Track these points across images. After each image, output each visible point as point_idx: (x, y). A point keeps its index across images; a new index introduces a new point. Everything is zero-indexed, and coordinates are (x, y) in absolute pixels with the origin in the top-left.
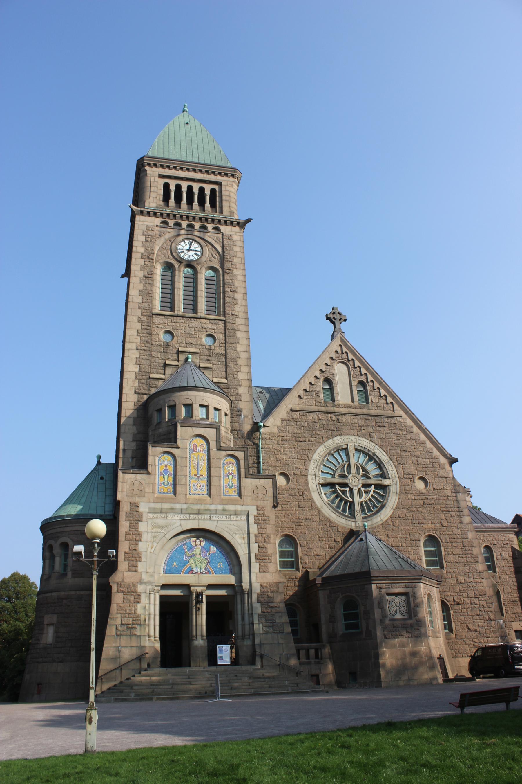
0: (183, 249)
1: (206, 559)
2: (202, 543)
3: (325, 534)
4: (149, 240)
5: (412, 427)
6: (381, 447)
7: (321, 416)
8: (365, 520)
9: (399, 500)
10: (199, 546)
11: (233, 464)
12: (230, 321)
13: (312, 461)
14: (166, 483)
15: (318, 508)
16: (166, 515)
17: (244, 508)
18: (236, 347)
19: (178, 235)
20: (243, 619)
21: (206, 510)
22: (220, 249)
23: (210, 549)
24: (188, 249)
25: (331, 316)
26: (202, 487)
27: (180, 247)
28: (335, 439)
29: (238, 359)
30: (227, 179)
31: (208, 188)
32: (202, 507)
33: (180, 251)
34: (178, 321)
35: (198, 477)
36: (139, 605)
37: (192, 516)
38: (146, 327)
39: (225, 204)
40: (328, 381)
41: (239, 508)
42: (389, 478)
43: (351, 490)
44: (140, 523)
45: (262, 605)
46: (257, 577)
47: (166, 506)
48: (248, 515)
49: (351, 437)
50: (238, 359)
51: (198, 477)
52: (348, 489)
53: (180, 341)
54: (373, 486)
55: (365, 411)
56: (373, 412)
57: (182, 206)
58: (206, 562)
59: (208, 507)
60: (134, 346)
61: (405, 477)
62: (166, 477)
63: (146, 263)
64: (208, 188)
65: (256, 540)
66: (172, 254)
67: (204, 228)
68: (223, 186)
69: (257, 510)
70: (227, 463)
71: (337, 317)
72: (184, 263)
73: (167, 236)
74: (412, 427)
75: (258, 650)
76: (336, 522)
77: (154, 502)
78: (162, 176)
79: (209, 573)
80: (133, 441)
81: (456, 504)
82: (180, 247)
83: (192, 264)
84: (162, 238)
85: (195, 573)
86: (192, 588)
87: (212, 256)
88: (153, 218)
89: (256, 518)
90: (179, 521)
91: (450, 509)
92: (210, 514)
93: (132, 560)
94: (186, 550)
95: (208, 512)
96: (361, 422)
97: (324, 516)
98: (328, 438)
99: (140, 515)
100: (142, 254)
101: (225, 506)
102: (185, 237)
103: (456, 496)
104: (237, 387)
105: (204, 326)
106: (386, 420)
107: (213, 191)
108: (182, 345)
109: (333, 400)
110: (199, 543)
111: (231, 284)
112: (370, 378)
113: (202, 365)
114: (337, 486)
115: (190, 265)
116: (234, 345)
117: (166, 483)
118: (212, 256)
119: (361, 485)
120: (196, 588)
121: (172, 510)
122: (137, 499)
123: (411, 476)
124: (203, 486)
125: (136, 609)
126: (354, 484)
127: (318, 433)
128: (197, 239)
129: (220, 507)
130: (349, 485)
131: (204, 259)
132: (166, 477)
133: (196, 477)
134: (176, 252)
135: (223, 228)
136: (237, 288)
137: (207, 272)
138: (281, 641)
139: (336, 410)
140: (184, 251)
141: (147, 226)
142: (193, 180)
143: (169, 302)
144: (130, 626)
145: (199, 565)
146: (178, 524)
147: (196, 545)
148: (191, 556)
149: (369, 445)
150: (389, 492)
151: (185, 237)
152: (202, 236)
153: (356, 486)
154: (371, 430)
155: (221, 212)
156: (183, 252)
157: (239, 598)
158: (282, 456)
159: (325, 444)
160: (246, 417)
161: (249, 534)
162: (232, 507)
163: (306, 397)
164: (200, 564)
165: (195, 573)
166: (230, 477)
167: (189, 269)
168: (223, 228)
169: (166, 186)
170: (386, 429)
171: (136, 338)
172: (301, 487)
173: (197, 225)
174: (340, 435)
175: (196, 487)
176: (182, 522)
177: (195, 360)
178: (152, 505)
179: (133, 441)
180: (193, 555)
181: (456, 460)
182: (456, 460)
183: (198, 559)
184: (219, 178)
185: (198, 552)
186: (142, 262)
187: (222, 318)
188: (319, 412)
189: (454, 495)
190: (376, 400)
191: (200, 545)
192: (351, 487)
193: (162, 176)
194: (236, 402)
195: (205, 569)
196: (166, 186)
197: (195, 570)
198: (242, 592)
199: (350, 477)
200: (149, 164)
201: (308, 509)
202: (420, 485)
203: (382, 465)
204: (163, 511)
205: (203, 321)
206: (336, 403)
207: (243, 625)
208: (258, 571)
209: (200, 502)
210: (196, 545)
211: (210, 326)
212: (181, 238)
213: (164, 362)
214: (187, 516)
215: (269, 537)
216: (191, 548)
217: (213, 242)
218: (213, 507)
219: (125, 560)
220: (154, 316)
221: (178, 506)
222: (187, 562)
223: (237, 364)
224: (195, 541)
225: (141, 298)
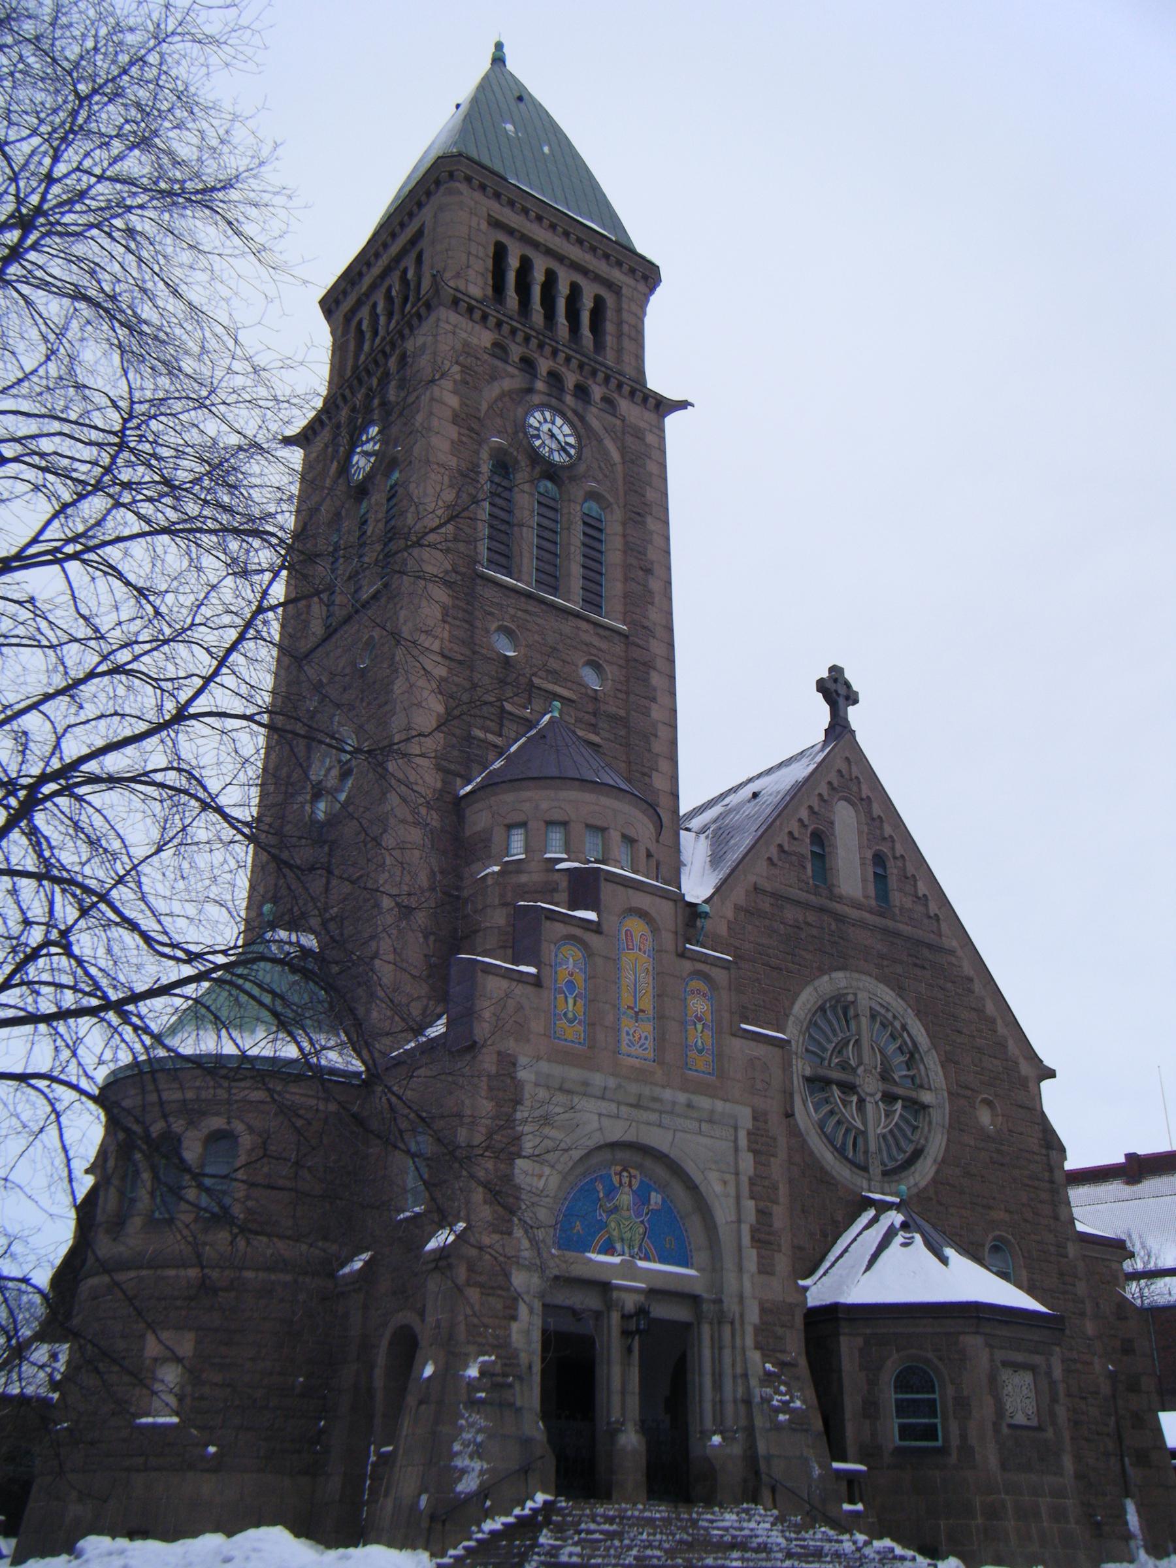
0: (537, 429)
1: (642, 1222)
2: (634, 1181)
4: (468, 378)
5: (970, 980)
6: (918, 1014)
7: (811, 917)
8: (886, 1179)
9: (947, 1145)
10: (627, 1189)
11: (704, 995)
13: (792, 1018)
14: (570, 1015)
15: (800, 1134)
16: (569, 1097)
18: (648, 709)
19: (530, 390)
20: (718, 1385)
21: (655, 1099)
23: (649, 1200)
24: (552, 432)
25: (831, 686)
26: (642, 1041)
27: (532, 421)
28: (835, 975)
29: (652, 738)
30: (631, 282)
32: (647, 1091)
33: (532, 432)
36: (515, 1326)
37: (623, 1109)
38: (461, 604)
39: (626, 343)
40: (819, 838)
41: (719, 1105)
42: (930, 1089)
43: (861, 1102)
47: (574, 1074)
48: (736, 1129)
49: (864, 977)
50: (652, 738)
51: (637, 1013)
52: (855, 1099)
54: (900, 1102)
58: (641, 1230)
59: (658, 1091)
60: (436, 647)
61: (959, 1093)
62: (571, 1001)
63: (464, 439)
65: (751, 1191)
69: (755, 1119)
70: (692, 992)
71: (842, 691)
73: (507, 384)
75: (763, 1467)
76: (834, 1173)
77: (549, 1060)
78: (496, 224)
80: (433, 889)
81: (1047, 1174)
84: (496, 384)
86: (615, 1294)
87: (600, 467)
88: (477, 327)
90: (596, 1117)
91: (1036, 1183)
92: (661, 1112)
94: (601, 1195)
95: (657, 1106)
97: (812, 1154)
98: (822, 971)
99: (518, 1085)
101: (692, 1097)
102: (545, 399)
103: (1048, 1155)
105: (585, 637)
106: (926, 952)
107: (599, 301)
110: (627, 1180)
114: (834, 1087)
115: (551, 472)
118: (600, 467)
119: (879, 1096)
120: (624, 1295)
121: (585, 1089)
122: (511, 1045)
123: (969, 1093)
124: (646, 1038)
125: (509, 1336)
126: (868, 1090)
127: (803, 953)
128: (570, 414)
129: (682, 1098)
130: (859, 1090)
131: (582, 468)
132: (571, 1001)
133: (630, 1012)
134: (525, 433)
135: (624, 405)
136: (652, 563)
137: (586, 505)
139: (838, 907)
141: (466, 344)
144: (500, 1379)
145: (628, 1235)
146: (596, 1125)
147: (621, 1184)
149: (894, 1004)
150: (930, 1123)
151: (545, 399)
152: (580, 410)
153: (872, 1095)
156: (538, 437)
157: (706, 1330)
159: (816, 983)
161: (737, 1174)
162: (704, 1102)
163: (780, 863)
166: (699, 1027)
167: (549, 485)
169: (500, 253)
174: (843, 968)
176: (606, 1122)
177: (567, 718)
180: (616, 1209)
181: (1051, 1074)
182: (1051, 1074)
183: (626, 1219)
184: (616, 275)
185: (626, 1203)
186: (453, 432)
188: (807, 906)
189: (1044, 1151)
190: (908, 903)
191: (630, 1185)
192: (863, 1095)
193: (496, 224)
195: (640, 1249)
196: (500, 253)
198: (721, 1318)
199: (860, 1070)
200: (468, 179)
202: (985, 1117)
203: (917, 1056)
204: (566, 1086)
205: (584, 625)
207: (719, 1404)
209: (641, 1076)
210: (621, 1184)
211: (596, 641)
212: (536, 399)
214: (613, 1107)
215: (775, 1188)
216: (611, 1191)
220: (478, 581)
221: (598, 1079)
223: (649, 751)
224: (620, 1174)
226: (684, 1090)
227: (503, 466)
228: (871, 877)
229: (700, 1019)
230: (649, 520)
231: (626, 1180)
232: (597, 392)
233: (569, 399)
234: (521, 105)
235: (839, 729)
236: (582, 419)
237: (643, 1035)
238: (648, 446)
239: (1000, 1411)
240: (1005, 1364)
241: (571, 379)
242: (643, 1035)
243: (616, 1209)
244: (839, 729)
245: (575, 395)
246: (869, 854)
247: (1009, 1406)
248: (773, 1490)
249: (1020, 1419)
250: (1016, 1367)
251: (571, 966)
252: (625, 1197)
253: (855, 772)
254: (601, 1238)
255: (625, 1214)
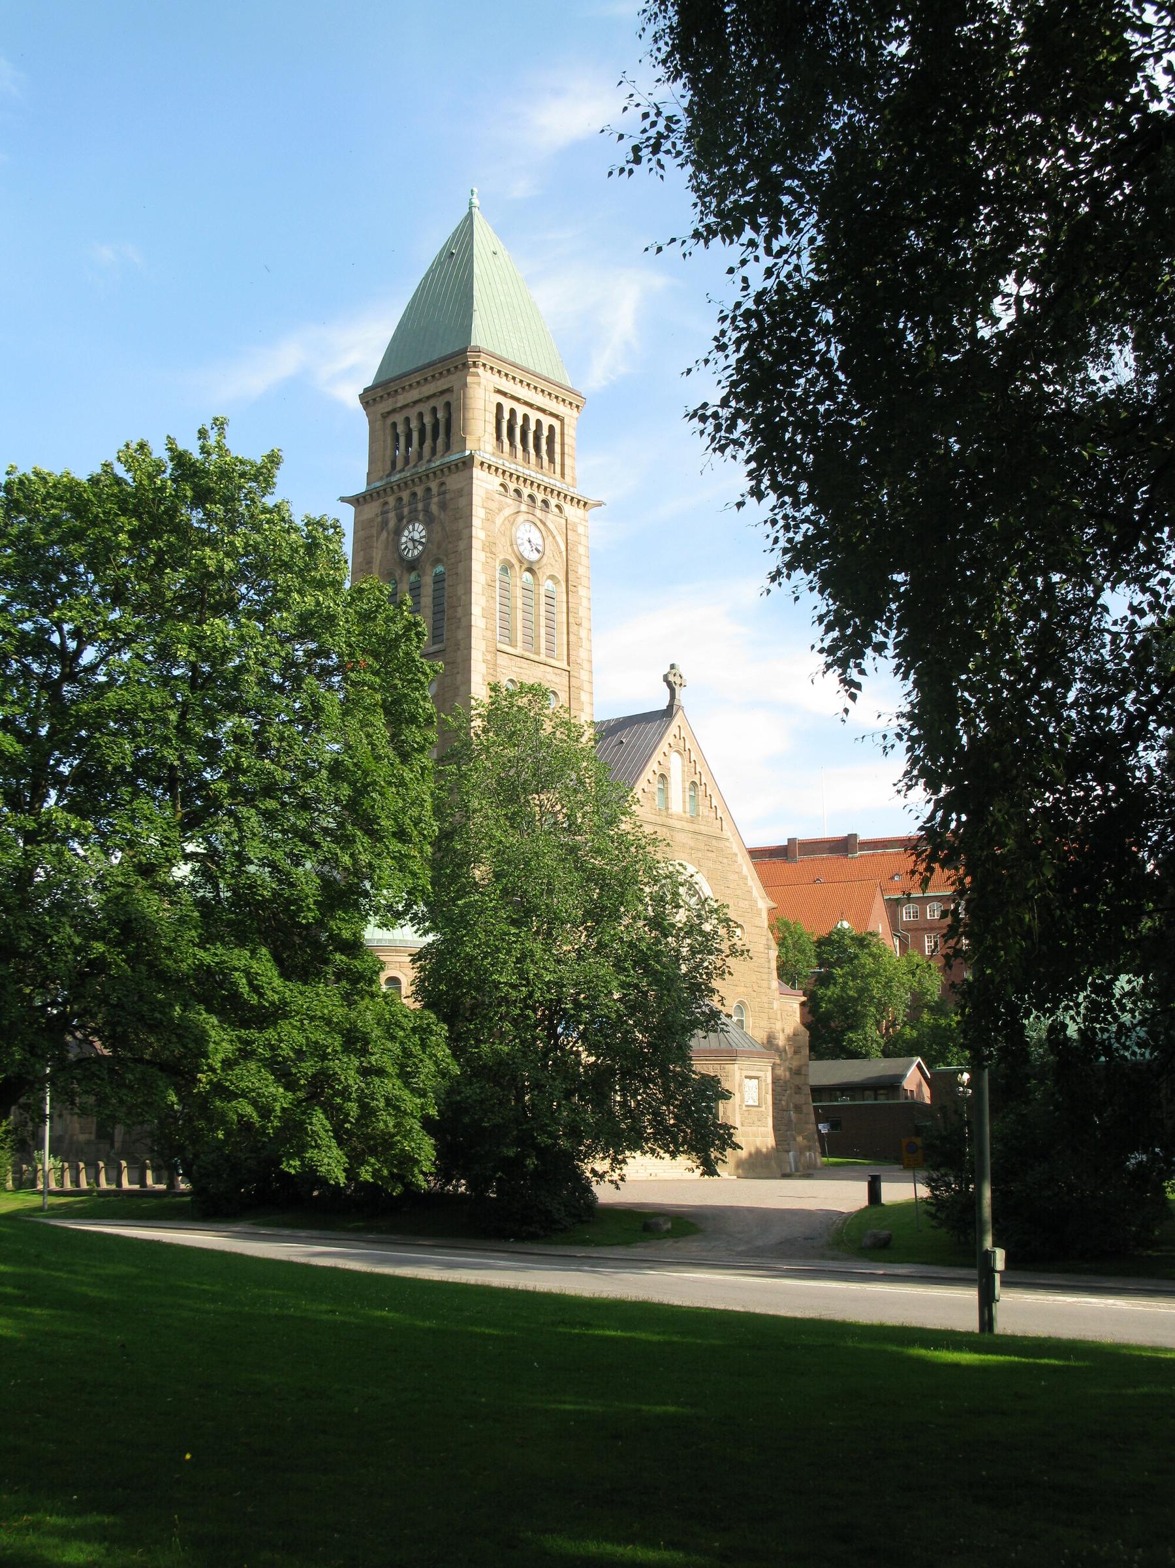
5: (736, 855)
22: (563, 548)
34: (525, 666)
55: (695, 827)
56: (703, 829)
66: (512, 545)
72: (525, 566)
74: (736, 855)
96: (691, 843)
102: (526, 516)
106: (714, 842)
107: (551, 428)
109: (667, 808)
128: (539, 523)
135: (567, 507)
154: (700, 855)
155: (563, 475)
168: (567, 507)
169: (499, 407)
170: (713, 855)
184: (560, 409)
187: (564, 665)
196: (499, 407)
200: (484, 365)
206: (670, 811)
217: (555, 533)
227: (506, 568)
228: (688, 799)
230: (580, 588)
232: (553, 502)
233: (538, 513)
234: (493, 249)
236: (544, 524)
238: (579, 535)
239: (742, 1100)
240: (747, 1077)
247: (746, 1098)
249: (751, 1103)
250: (750, 1078)
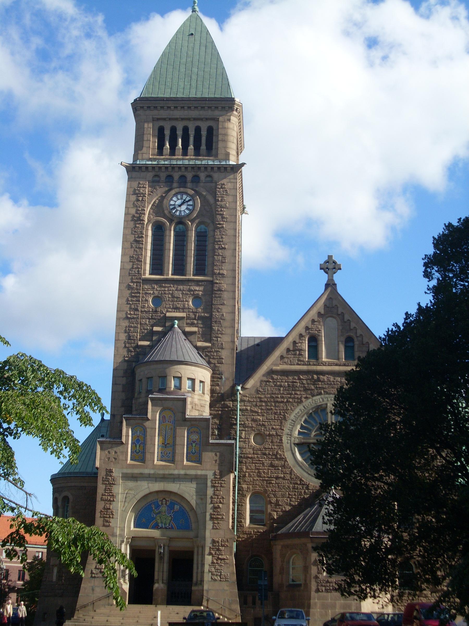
1: (171, 516)
2: (167, 502)
3: (295, 491)
4: (140, 198)
10: (165, 505)
11: (197, 432)
12: (217, 281)
14: (138, 451)
17: (203, 472)
26: (168, 454)
27: (172, 203)
31: (204, 127)
33: (171, 207)
35: (166, 445)
44: (114, 486)
45: (213, 557)
46: (210, 533)
53: (168, 306)
57: (177, 152)
59: (172, 472)
62: (138, 446)
64: (204, 127)
65: (212, 501)
67: (196, 179)
68: (220, 123)
79: (172, 528)
80: (122, 406)
82: (172, 203)
83: (183, 220)
85: (160, 528)
89: (214, 482)
93: (107, 517)
100: (134, 216)
104: (220, 350)
108: (170, 310)
111: (221, 240)
112: (359, 332)
113: (188, 329)
115: (180, 221)
116: (220, 307)
117: (138, 451)
124: (169, 453)
132: (138, 446)
138: (226, 588)
140: (176, 206)
142: (189, 119)
143: (158, 266)
146: (147, 487)
147: (162, 504)
148: (158, 514)
151: (177, 190)
156: (174, 208)
158: (259, 417)
160: (227, 379)
164: (165, 520)
165: (160, 528)
166: (194, 445)
171: (126, 307)
172: (276, 447)
173: (189, 176)
175: (163, 454)
178: (125, 471)
179: (122, 406)
180: (160, 512)
191: (166, 504)
194: (218, 365)
195: (169, 525)
197: (160, 525)
200: (142, 107)
201: (280, 468)
207: (197, 573)
208: (211, 527)
210: (162, 504)
212: (173, 192)
213: (151, 328)
216: (158, 507)
218: (176, 472)
219: (101, 517)
222: (154, 518)
224: (162, 501)
225: (131, 263)
226: (183, 469)
229: (194, 442)
231: (164, 502)
235: (331, 285)
237: (168, 453)
241: (189, 176)
242: (168, 453)
243: (160, 512)
244: (331, 285)
245: (192, 182)
246: (343, 339)
248: (208, 600)
251: (138, 433)
252: (163, 508)
253: (335, 302)
254: (153, 523)
255: (164, 514)
